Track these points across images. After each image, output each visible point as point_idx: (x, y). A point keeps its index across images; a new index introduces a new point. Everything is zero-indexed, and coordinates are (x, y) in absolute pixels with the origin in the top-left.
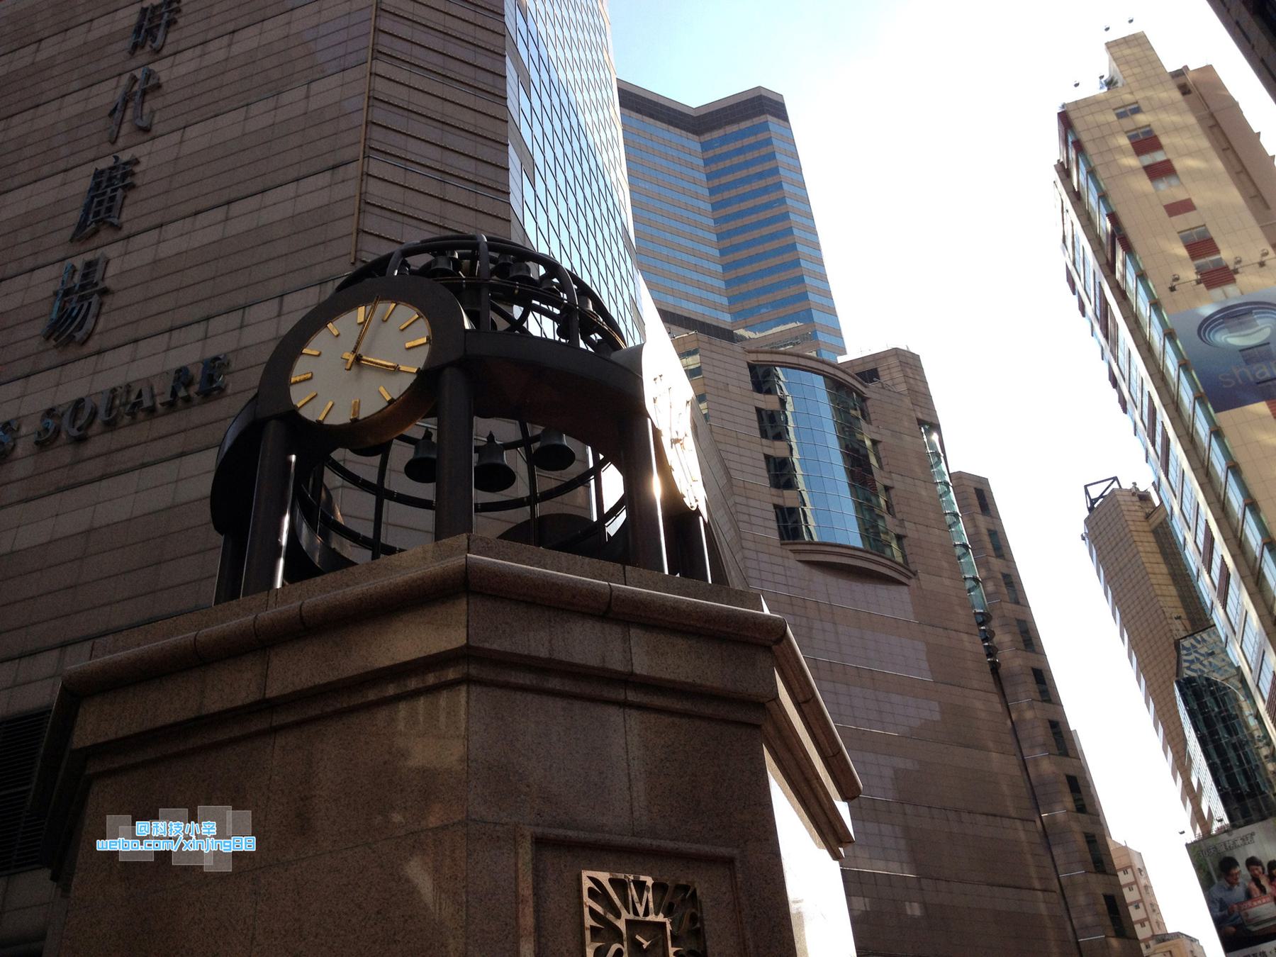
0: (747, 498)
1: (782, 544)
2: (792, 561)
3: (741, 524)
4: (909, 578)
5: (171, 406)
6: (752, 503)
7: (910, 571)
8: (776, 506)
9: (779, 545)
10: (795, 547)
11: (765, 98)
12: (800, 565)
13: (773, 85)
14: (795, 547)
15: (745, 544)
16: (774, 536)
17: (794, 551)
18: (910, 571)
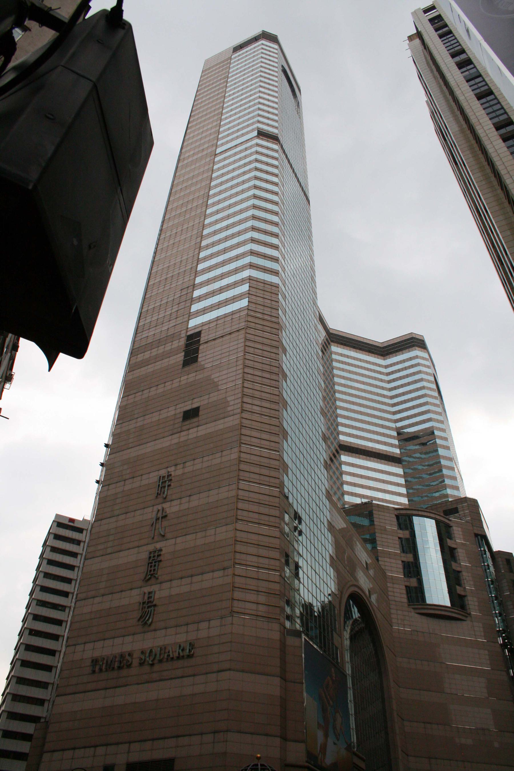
0: (393, 583)
1: (409, 605)
2: (413, 614)
3: (390, 597)
4: (467, 617)
5: (178, 658)
6: (395, 586)
7: (467, 614)
8: (406, 586)
9: (407, 606)
10: (415, 607)
11: (415, 338)
12: (416, 614)
13: (418, 330)
14: (415, 607)
15: (392, 606)
16: (405, 600)
17: (414, 609)
18: (467, 614)
